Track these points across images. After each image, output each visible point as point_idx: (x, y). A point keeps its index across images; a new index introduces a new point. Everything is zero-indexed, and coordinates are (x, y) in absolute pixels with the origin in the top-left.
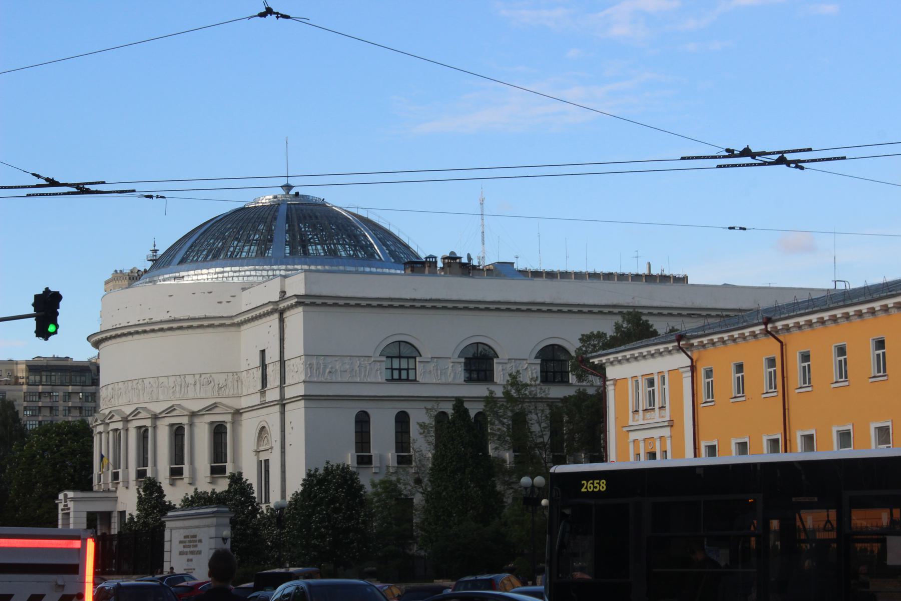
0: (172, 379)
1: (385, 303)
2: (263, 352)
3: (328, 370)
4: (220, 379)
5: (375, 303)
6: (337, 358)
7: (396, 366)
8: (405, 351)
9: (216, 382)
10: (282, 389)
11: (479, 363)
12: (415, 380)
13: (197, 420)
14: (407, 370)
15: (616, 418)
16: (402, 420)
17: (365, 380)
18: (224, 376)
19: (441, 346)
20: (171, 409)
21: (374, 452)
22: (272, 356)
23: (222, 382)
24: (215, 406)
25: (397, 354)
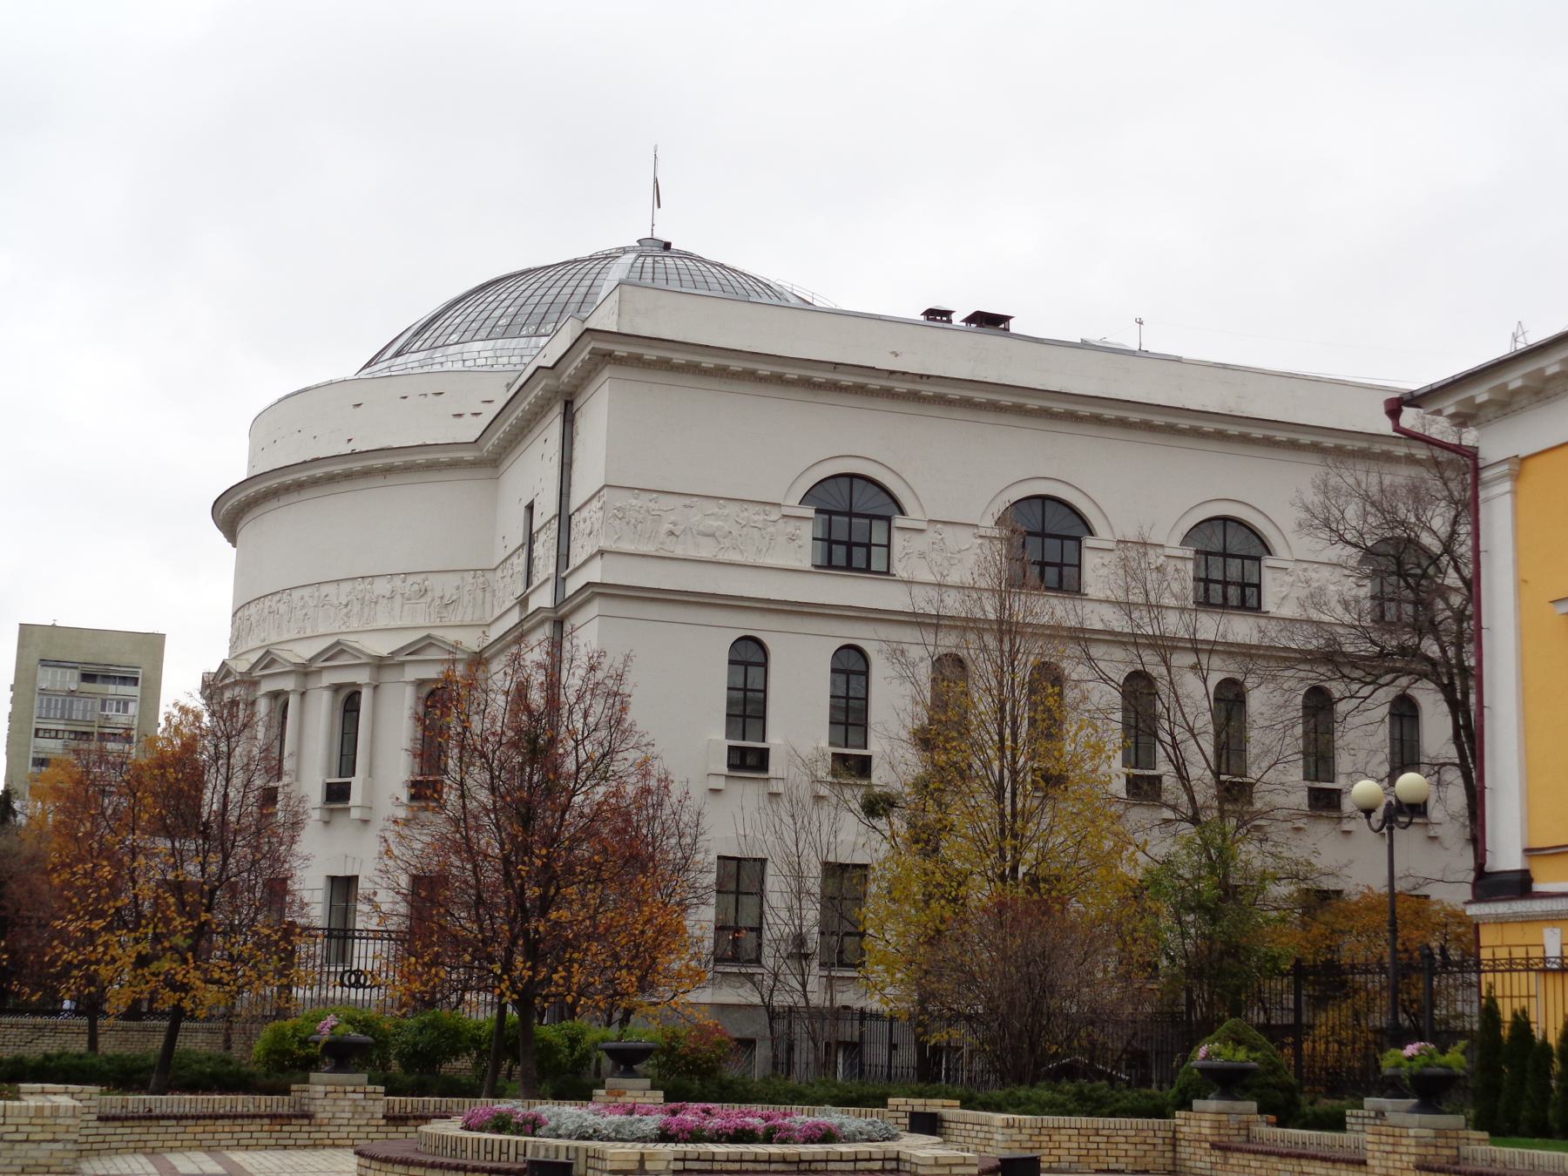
0: (346, 587)
1: (820, 376)
2: (530, 508)
3: (667, 527)
4: (445, 586)
5: (792, 373)
6: (687, 501)
7: (840, 533)
8: (865, 500)
9: (438, 593)
10: (560, 582)
11: (1046, 538)
12: (888, 573)
13: (388, 676)
14: (868, 546)
15: (1521, 583)
16: (851, 668)
17: (760, 561)
18: (454, 580)
19: (956, 495)
20: (337, 650)
21: (775, 739)
22: (547, 507)
23: (450, 593)
24: (428, 643)
25: (844, 507)
